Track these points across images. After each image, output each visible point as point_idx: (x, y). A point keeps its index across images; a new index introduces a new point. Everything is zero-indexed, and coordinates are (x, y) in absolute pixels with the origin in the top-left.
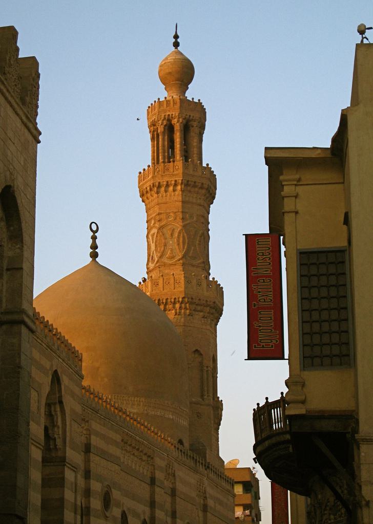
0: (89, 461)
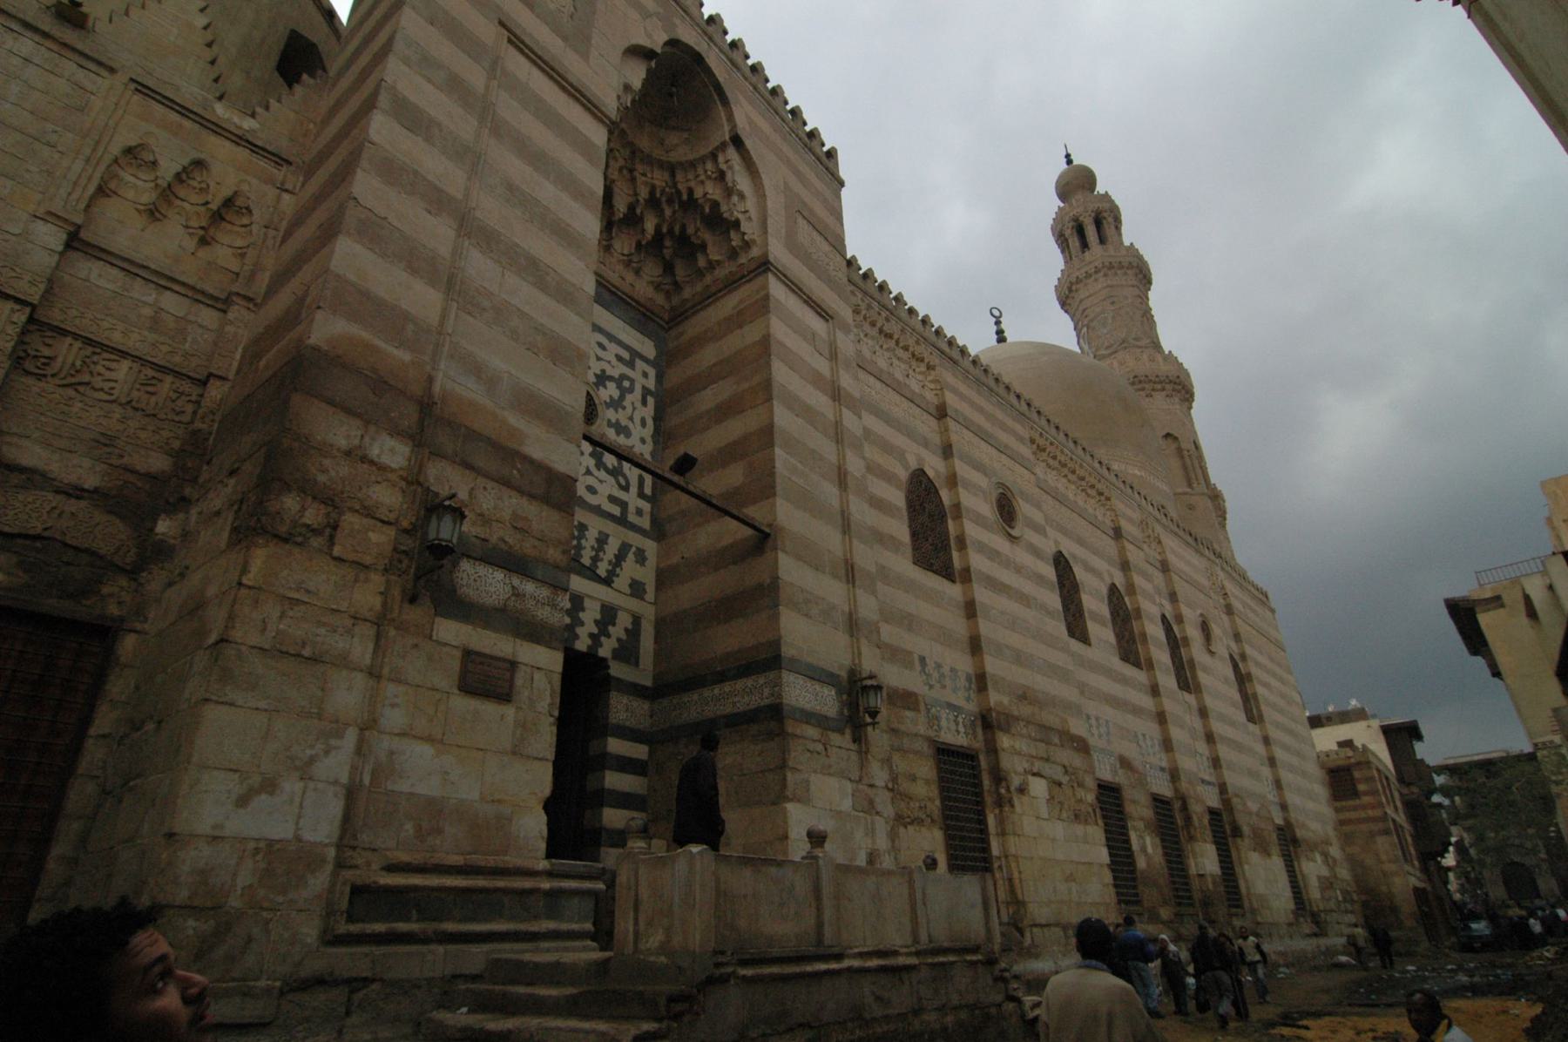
0: (947, 430)
